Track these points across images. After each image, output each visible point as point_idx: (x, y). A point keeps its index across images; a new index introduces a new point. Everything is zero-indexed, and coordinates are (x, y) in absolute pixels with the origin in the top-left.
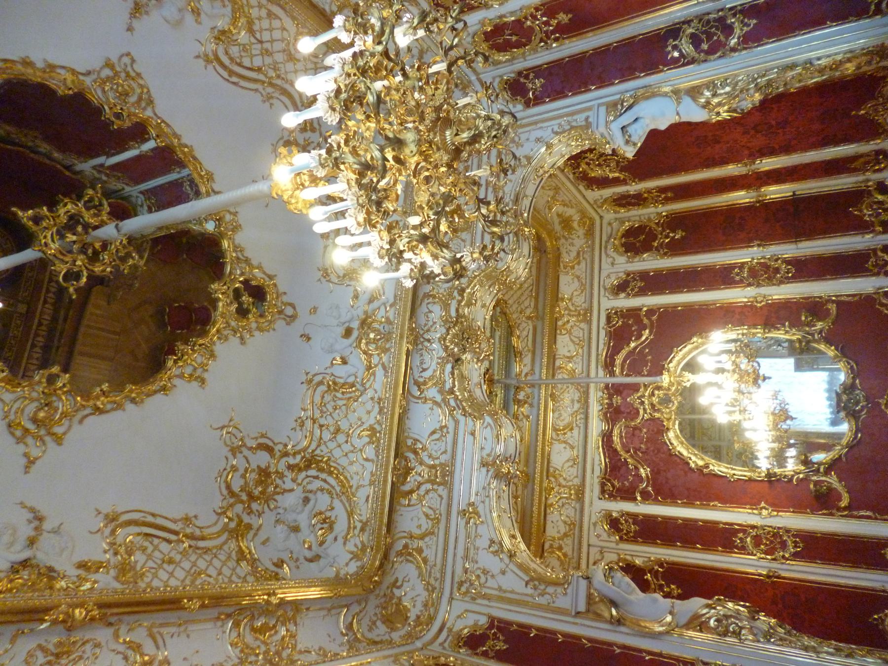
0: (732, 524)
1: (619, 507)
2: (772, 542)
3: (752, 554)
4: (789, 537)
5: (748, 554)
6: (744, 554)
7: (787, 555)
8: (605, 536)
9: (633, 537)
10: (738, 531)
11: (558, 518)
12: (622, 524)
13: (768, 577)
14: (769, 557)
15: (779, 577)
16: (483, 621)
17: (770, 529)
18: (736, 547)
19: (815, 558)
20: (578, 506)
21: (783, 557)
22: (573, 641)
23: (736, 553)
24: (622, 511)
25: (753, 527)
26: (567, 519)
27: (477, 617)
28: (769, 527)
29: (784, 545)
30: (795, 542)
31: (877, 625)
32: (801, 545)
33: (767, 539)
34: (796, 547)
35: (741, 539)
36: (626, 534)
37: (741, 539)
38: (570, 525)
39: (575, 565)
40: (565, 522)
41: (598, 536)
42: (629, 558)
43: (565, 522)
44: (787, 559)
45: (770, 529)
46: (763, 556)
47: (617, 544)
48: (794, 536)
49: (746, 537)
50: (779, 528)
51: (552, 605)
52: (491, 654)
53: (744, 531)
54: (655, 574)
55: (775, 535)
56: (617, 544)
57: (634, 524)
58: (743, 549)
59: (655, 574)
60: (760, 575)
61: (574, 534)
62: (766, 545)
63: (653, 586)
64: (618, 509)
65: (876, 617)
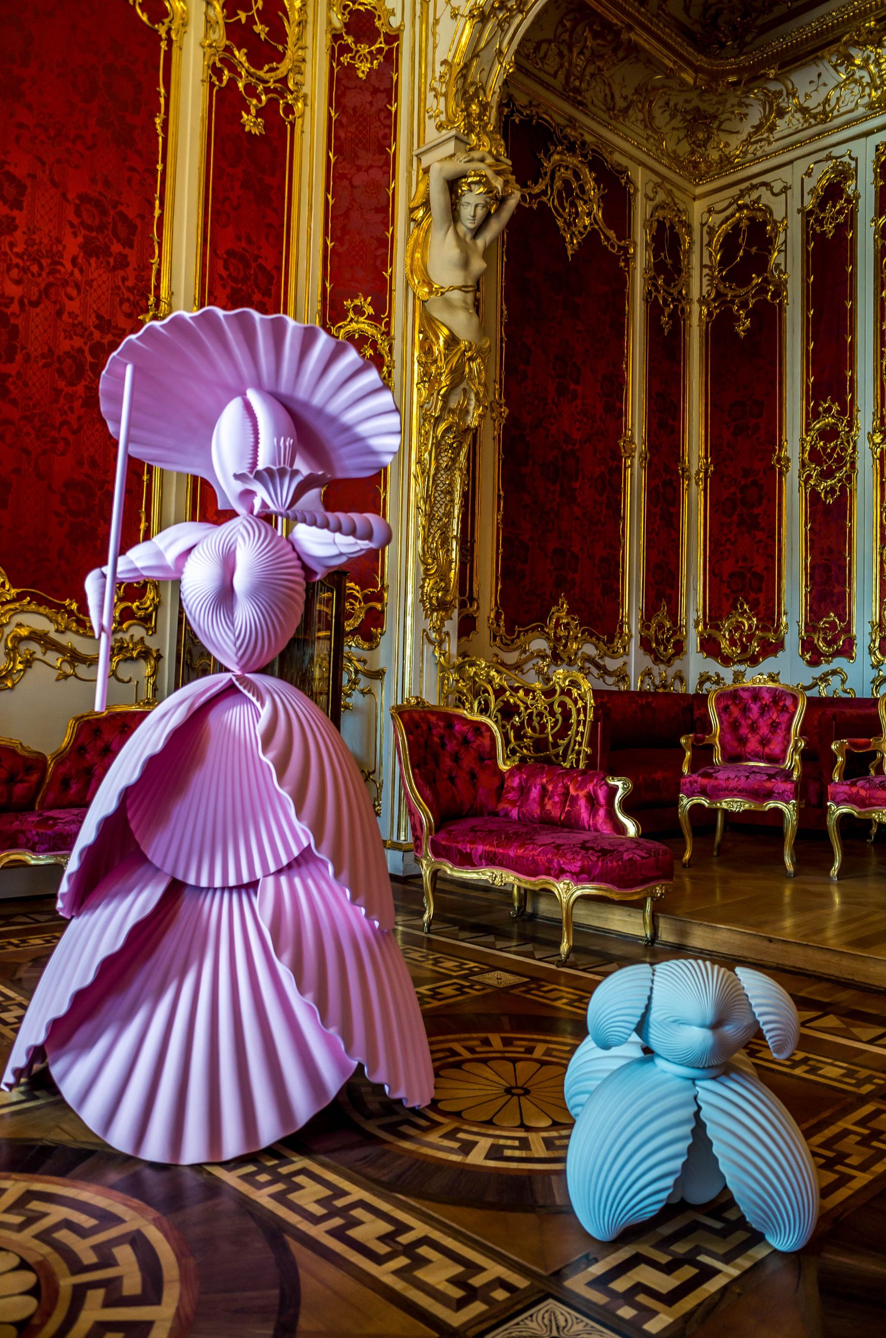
0: (852, 390)
1: (865, 187)
2: (830, 456)
3: (808, 430)
4: (840, 481)
5: (808, 425)
6: (807, 418)
7: (812, 482)
8: (810, 184)
9: (814, 230)
10: (843, 404)
11: (832, 83)
12: (834, 206)
13: (779, 460)
14: (806, 455)
15: (781, 474)
16: (395, 22)
17: (850, 451)
18: (817, 405)
19: (813, 521)
20: (861, 110)
21: (809, 477)
22: (387, 166)
23: (808, 404)
24: (857, 198)
25: (850, 424)
26: (833, 102)
27: (398, 12)
28: (854, 448)
29: (826, 475)
30: (832, 491)
31: (736, 609)
32: (830, 501)
33: (833, 449)
34: (826, 493)
35: (829, 410)
36: (817, 220)
37: (829, 410)
38: (824, 112)
39: (759, 153)
40: (827, 101)
41: (809, 174)
42: (781, 238)
43: (827, 101)
44: (806, 484)
45: (850, 451)
46: (808, 448)
47: (799, 211)
48: (843, 489)
49: (833, 416)
50: (853, 464)
51: (427, 115)
52: (345, 59)
53: (842, 413)
54: (762, 290)
55: (840, 459)
56: (799, 211)
57: (837, 227)
58: (813, 415)
59: (762, 290)
60: (781, 446)
61: (811, 126)
62: (824, 448)
63: (742, 291)
64: (860, 190)
65: (745, 607)
